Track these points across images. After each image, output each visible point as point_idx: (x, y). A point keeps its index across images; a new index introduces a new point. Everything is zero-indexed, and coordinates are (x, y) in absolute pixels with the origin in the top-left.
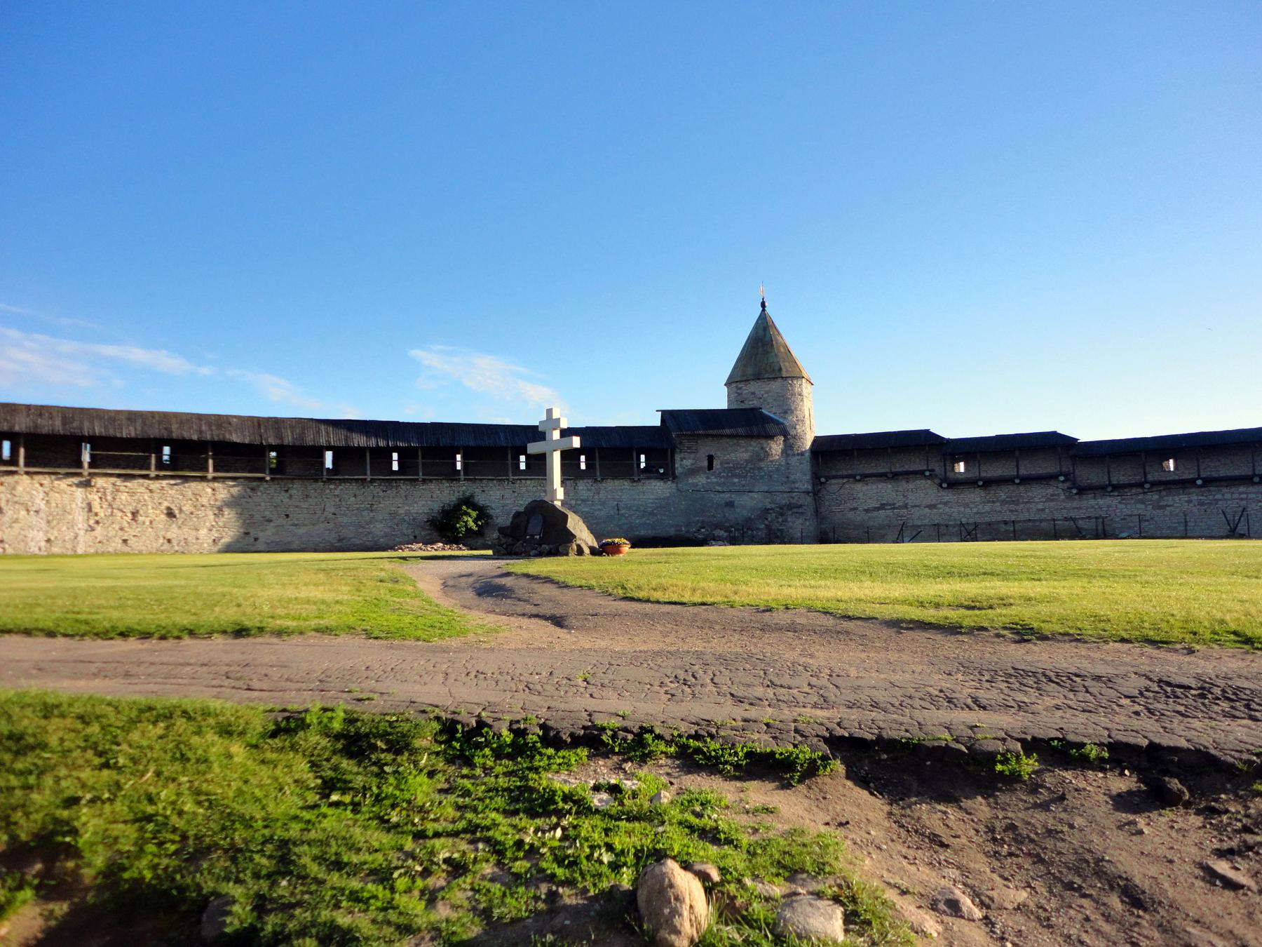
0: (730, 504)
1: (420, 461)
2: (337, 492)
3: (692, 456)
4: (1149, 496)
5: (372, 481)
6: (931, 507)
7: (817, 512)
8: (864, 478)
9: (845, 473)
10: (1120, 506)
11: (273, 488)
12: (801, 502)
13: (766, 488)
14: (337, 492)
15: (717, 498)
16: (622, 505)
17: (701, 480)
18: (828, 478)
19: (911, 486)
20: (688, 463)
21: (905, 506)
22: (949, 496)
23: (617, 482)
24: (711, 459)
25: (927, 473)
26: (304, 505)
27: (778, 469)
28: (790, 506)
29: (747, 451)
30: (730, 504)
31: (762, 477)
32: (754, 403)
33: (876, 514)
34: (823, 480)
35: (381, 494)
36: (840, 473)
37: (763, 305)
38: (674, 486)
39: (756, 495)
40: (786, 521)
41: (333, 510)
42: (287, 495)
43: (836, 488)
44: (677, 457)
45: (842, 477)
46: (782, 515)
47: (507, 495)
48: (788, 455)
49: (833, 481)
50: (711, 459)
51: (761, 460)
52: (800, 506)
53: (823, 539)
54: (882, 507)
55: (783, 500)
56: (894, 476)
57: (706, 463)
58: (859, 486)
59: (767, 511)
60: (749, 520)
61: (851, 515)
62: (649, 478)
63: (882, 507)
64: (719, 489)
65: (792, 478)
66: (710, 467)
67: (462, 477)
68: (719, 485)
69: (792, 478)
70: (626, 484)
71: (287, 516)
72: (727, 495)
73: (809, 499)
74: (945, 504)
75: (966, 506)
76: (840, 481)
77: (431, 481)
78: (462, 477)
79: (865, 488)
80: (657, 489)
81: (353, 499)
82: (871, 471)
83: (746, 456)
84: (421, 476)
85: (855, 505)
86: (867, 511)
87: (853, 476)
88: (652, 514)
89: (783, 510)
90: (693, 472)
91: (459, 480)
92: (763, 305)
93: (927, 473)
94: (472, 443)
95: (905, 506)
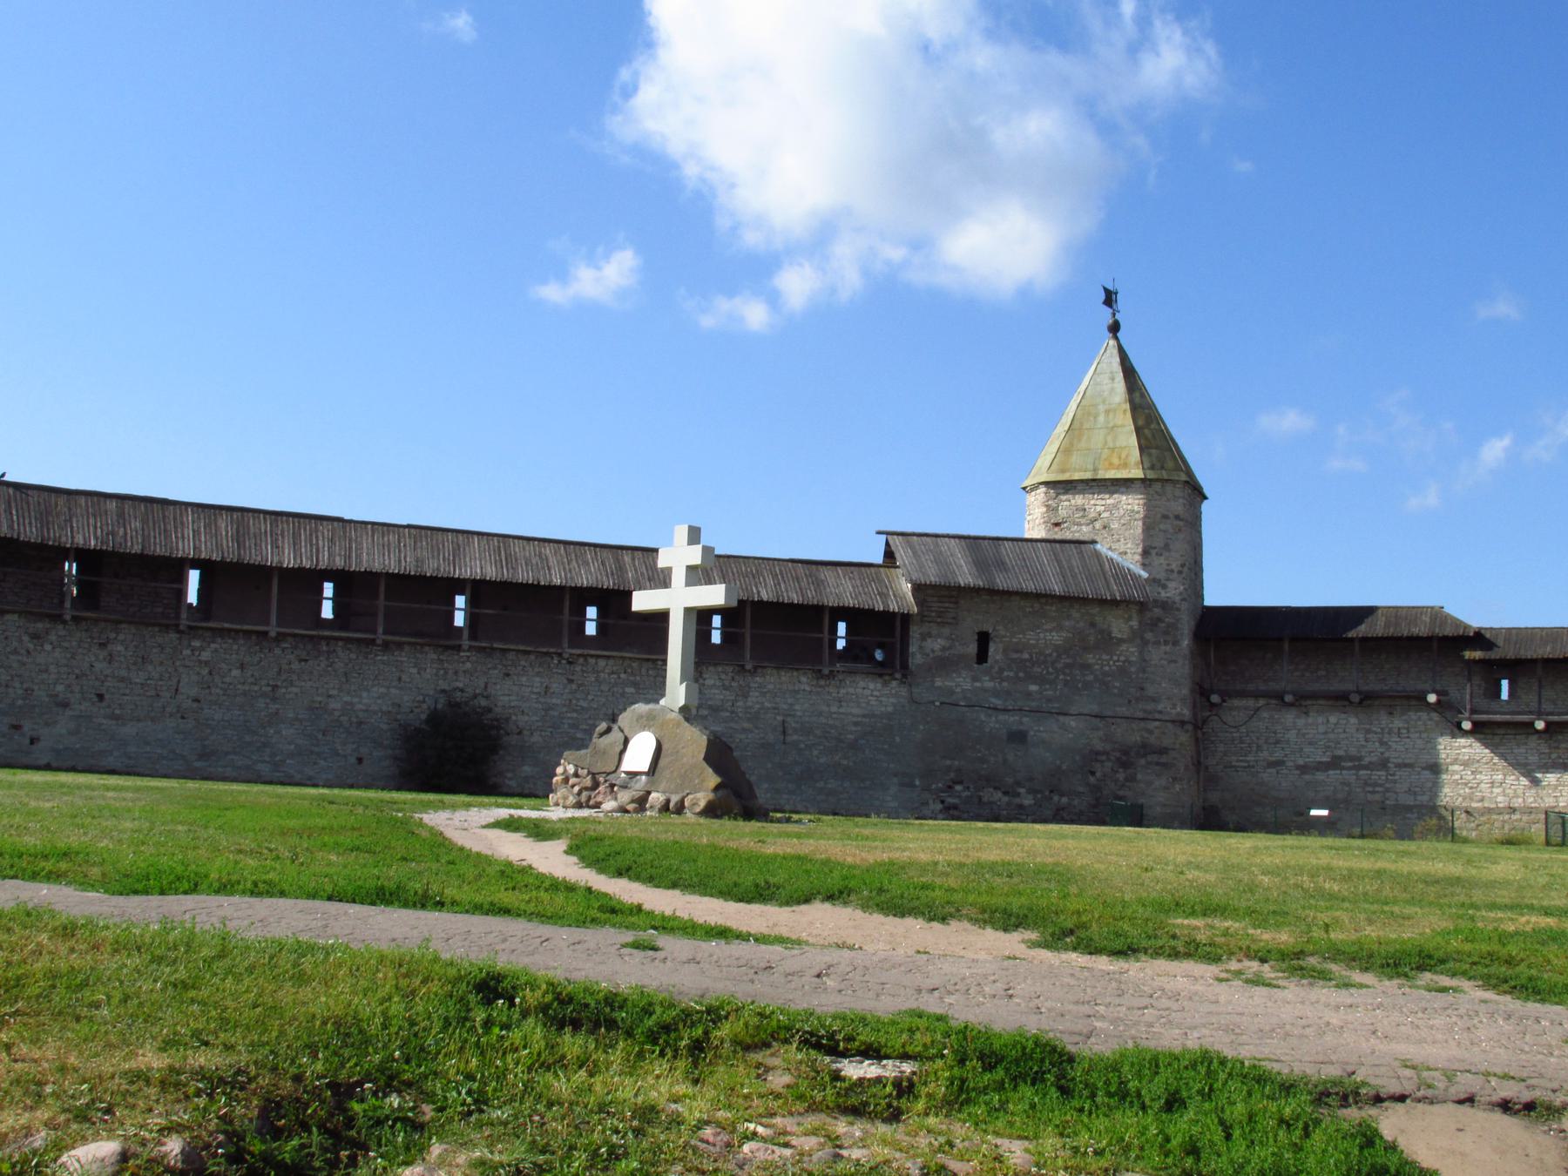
1: (381, 602)
2: (206, 655)
3: (946, 631)
5: (281, 637)
7: (1198, 764)
8: (1302, 700)
9: (1262, 687)
12: (1166, 742)
13: (1095, 708)
14: (206, 655)
15: (993, 723)
16: (791, 723)
17: (962, 682)
18: (1225, 695)
19: (1397, 723)
20: (936, 645)
21: (1383, 764)
23: (785, 676)
24: (984, 639)
25: (1432, 698)
26: (139, 678)
28: (1145, 749)
29: (1060, 628)
30: (1018, 737)
32: (1083, 533)
33: (1320, 776)
34: (1215, 698)
35: (296, 666)
36: (1251, 687)
38: (904, 691)
41: (194, 692)
42: (103, 654)
45: (1256, 695)
46: (1125, 765)
47: (555, 687)
48: (1145, 643)
49: (1236, 702)
50: (984, 639)
52: (1163, 751)
53: (1209, 819)
54: (1335, 763)
55: (1133, 735)
56: (1367, 700)
57: (972, 649)
58: (1289, 717)
59: (1095, 755)
61: (1268, 776)
62: (851, 673)
63: (1335, 763)
64: (997, 702)
65: (1151, 690)
66: (982, 656)
67: (466, 643)
68: (996, 694)
69: (1151, 690)
70: (805, 681)
71: (101, 697)
72: (1012, 719)
73: (1184, 737)
76: (1251, 703)
77: (400, 645)
78: (466, 643)
79: (1301, 722)
81: (236, 672)
82: (1316, 687)
83: (1056, 638)
84: (381, 637)
85: (1278, 755)
86: (1304, 769)
87: (1279, 697)
89: (1126, 758)
90: (944, 664)
91: (459, 648)
93: (1432, 698)
94: (491, 573)
95: (1383, 764)
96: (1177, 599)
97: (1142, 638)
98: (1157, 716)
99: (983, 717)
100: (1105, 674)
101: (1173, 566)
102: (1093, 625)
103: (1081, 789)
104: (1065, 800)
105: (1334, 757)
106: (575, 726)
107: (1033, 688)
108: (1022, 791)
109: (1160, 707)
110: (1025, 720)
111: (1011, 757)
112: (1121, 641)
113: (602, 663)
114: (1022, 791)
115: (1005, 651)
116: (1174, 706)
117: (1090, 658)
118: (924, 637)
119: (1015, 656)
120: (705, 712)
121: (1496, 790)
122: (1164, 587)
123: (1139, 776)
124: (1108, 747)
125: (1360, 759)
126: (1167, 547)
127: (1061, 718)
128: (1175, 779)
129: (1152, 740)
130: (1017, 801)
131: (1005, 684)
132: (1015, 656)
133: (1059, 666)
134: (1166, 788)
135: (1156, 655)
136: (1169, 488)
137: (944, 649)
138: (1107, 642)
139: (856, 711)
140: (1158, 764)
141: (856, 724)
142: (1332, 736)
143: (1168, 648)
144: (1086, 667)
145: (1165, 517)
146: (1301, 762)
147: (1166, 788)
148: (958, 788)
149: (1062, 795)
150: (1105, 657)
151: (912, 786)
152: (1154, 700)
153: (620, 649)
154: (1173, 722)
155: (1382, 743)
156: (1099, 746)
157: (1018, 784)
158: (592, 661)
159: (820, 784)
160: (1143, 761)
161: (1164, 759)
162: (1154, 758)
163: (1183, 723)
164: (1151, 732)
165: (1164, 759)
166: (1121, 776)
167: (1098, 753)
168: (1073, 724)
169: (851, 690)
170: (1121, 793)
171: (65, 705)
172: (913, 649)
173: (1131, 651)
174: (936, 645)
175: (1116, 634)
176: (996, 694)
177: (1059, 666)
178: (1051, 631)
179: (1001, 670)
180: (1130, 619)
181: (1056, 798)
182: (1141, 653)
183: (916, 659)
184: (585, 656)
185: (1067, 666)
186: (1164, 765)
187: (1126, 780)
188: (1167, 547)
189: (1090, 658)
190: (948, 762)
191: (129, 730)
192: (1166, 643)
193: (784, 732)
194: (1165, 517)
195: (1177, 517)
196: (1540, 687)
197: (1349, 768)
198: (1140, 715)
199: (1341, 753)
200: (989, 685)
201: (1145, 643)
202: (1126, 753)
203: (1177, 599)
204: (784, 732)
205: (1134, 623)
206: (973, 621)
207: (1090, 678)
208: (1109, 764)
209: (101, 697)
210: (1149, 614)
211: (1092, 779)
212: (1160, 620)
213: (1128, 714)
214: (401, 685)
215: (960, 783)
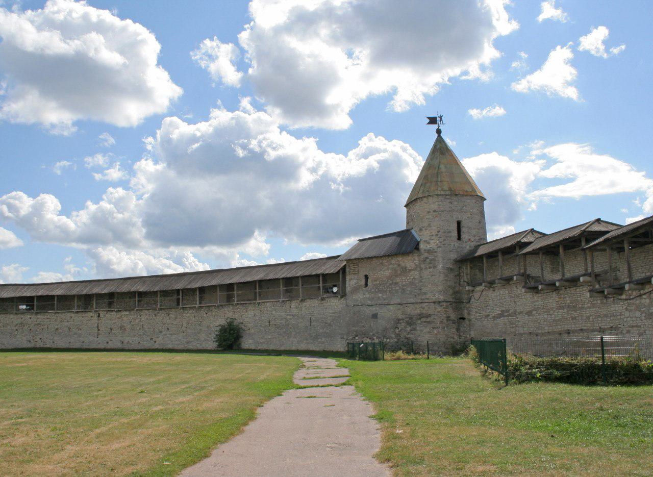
0: (375, 316)
3: (356, 276)
4: (643, 301)
5: (201, 307)
6: (529, 313)
10: (627, 314)
11: (162, 314)
12: (430, 312)
13: (399, 301)
16: (313, 318)
20: (353, 282)
21: (515, 313)
22: (538, 300)
24: (367, 277)
27: (412, 283)
28: (421, 316)
29: (388, 269)
30: (375, 316)
31: (397, 291)
33: (498, 321)
37: (439, 132)
39: (391, 308)
40: (415, 329)
42: (168, 317)
43: (479, 294)
44: (348, 278)
48: (421, 269)
49: (479, 288)
50: (367, 277)
51: (397, 276)
52: (429, 316)
57: (363, 282)
59: (398, 321)
60: (385, 330)
64: (369, 302)
66: (366, 285)
71: (168, 329)
72: (373, 309)
74: (536, 309)
75: (548, 312)
80: (334, 305)
81: (194, 319)
83: (387, 273)
86: (494, 317)
88: (330, 325)
90: (356, 290)
92: (439, 132)
96: (435, 247)
97: (420, 267)
98: (426, 301)
99: (366, 309)
100: (403, 286)
101: (434, 233)
102: (399, 265)
103: (393, 336)
104: (388, 340)
105: (503, 311)
106: (261, 326)
107: (380, 295)
108: (375, 338)
109: (427, 297)
110: (378, 308)
111: (372, 325)
112: (410, 270)
113: (268, 304)
114: (375, 338)
115: (372, 281)
116: (434, 295)
117: (398, 280)
118: (350, 280)
119: (375, 283)
120: (291, 317)
121: (545, 323)
122: (429, 243)
123: (418, 328)
124: (403, 317)
125: (508, 311)
126: (429, 225)
127: (388, 306)
128: (433, 328)
129: (424, 312)
130: (373, 341)
131: (372, 295)
132: (375, 283)
133: (388, 284)
134: (429, 332)
135: (426, 273)
136: (430, 199)
137: (356, 284)
138: (405, 271)
139: (331, 311)
140: (425, 322)
141: (331, 316)
142: (501, 301)
143: (431, 270)
144: (397, 284)
145: (429, 212)
146: (493, 315)
147: (429, 332)
148: (357, 338)
149: (387, 339)
150: (404, 278)
151: (343, 338)
152: (425, 294)
153: (268, 299)
154: (434, 302)
155: (515, 302)
156: (400, 317)
157: (374, 335)
158: (265, 303)
159: (320, 340)
160: (419, 322)
161: (428, 320)
162: (424, 320)
163: (440, 302)
164: (424, 308)
165: (428, 320)
166: (409, 329)
167: (399, 320)
168: (392, 308)
169: (329, 304)
170: (408, 336)
171: (161, 332)
172: (347, 285)
173: (415, 274)
174: (353, 282)
175: (408, 267)
176: (369, 299)
177: (388, 284)
178: (384, 271)
179: (371, 289)
180: (414, 260)
181: (385, 340)
182: (420, 274)
183: (348, 289)
184: (264, 302)
185: (390, 284)
186: (429, 322)
187: (411, 330)
188: (429, 225)
189: (398, 280)
190: (354, 328)
191: (174, 337)
192: (430, 268)
193: (311, 322)
194: (429, 212)
195: (435, 211)
196: (541, 264)
197: (506, 316)
198: (419, 301)
199: (504, 309)
200: (368, 296)
201: (421, 269)
202: (411, 318)
203: (435, 247)
204: (311, 322)
205: (417, 262)
206: (364, 270)
207: (398, 288)
208: (403, 324)
209: (168, 329)
210: (422, 257)
211: (397, 331)
212: (427, 258)
213: (413, 301)
214: (218, 318)
215: (357, 336)
